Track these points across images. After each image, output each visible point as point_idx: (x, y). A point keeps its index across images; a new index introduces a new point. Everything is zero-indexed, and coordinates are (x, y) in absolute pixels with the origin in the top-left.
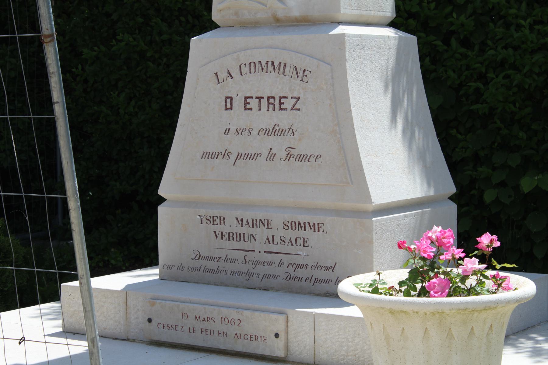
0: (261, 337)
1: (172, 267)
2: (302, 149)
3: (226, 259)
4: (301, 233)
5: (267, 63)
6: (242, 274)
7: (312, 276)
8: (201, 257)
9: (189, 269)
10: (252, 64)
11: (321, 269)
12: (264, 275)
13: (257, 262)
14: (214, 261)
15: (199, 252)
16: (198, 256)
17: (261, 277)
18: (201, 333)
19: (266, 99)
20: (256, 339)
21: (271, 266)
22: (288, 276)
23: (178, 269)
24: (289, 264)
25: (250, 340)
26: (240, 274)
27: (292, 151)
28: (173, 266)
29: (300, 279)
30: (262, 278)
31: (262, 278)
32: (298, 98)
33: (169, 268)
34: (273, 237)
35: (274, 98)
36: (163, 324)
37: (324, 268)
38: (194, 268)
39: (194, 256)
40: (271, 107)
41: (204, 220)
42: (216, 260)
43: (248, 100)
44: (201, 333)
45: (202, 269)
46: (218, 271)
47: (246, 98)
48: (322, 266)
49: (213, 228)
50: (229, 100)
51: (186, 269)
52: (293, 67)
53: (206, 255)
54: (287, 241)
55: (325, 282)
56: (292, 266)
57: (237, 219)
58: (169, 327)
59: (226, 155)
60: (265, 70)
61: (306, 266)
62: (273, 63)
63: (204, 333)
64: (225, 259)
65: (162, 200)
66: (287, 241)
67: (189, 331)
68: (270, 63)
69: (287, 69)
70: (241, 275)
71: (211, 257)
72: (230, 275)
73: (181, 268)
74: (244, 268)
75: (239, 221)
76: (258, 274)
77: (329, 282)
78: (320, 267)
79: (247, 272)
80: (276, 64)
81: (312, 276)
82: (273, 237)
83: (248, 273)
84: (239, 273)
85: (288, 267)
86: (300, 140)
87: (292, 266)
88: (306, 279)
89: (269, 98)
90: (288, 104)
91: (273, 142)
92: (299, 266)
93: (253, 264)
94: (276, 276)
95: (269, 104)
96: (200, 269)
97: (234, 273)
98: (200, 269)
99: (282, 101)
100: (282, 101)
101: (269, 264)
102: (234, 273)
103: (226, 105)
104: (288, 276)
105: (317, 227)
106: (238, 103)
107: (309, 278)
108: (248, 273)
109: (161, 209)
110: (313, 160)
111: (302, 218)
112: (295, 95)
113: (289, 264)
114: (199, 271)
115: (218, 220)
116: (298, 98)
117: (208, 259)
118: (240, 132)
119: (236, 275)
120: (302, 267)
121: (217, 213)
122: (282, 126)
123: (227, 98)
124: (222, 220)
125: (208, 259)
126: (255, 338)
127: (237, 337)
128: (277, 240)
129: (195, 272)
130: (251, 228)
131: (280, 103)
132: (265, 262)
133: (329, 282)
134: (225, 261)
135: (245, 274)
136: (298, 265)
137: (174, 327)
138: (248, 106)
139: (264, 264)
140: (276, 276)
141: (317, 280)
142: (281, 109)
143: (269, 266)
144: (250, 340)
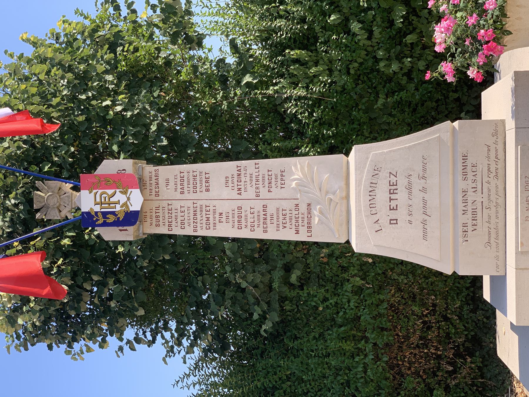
2: (419, 168)
4: (469, 168)
5: (370, 195)
10: (371, 206)
17: (498, 197)
19: (391, 195)
26: (497, 212)
27: (421, 175)
29: (497, 169)
32: (390, 173)
34: (472, 188)
35: (390, 190)
39: (489, 247)
40: (395, 191)
41: (466, 239)
42: (490, 230)
43: (392, 208)
45: (496, 241)
46: (496, 229)
47: (390, 210)
49: (470, 233)
50: (392, 222)
52: (373, 178)
53: (487, 238)
54: (474, 178)
57: (463, 214)
59: (424, 222)
60: (374, 197)
62: (370, 192)
65: (454, 272)
66: (474, 178)
68: (371, 194)
69: (374, 182)
74: (493, 209)
75: (465, 212)
80: (371, 189)
82: (472, 188)
86: (414, 171)
89: (390, 194)
90: (393, 179)
91: (415, 190)
92: (489, 170)
95: (393, 193)
99: (392, 184)
100: (392, 184)
103: (395, 224)
105: (465, 158)
106: (393, 215)
109: (461, 273)
110: (425, 162)
111: (460, 168)
112: (388, 175)
115: (465, 228)
116: (390, 173)
118: (411, 213)
121: (460, 229)
122: (406, 183)
123: (390, 223)
124: (465, 225)
128: (474, 185)
130: (468, 204)
131: (393, 185)
138: (395, 208)
142: (396, 185)
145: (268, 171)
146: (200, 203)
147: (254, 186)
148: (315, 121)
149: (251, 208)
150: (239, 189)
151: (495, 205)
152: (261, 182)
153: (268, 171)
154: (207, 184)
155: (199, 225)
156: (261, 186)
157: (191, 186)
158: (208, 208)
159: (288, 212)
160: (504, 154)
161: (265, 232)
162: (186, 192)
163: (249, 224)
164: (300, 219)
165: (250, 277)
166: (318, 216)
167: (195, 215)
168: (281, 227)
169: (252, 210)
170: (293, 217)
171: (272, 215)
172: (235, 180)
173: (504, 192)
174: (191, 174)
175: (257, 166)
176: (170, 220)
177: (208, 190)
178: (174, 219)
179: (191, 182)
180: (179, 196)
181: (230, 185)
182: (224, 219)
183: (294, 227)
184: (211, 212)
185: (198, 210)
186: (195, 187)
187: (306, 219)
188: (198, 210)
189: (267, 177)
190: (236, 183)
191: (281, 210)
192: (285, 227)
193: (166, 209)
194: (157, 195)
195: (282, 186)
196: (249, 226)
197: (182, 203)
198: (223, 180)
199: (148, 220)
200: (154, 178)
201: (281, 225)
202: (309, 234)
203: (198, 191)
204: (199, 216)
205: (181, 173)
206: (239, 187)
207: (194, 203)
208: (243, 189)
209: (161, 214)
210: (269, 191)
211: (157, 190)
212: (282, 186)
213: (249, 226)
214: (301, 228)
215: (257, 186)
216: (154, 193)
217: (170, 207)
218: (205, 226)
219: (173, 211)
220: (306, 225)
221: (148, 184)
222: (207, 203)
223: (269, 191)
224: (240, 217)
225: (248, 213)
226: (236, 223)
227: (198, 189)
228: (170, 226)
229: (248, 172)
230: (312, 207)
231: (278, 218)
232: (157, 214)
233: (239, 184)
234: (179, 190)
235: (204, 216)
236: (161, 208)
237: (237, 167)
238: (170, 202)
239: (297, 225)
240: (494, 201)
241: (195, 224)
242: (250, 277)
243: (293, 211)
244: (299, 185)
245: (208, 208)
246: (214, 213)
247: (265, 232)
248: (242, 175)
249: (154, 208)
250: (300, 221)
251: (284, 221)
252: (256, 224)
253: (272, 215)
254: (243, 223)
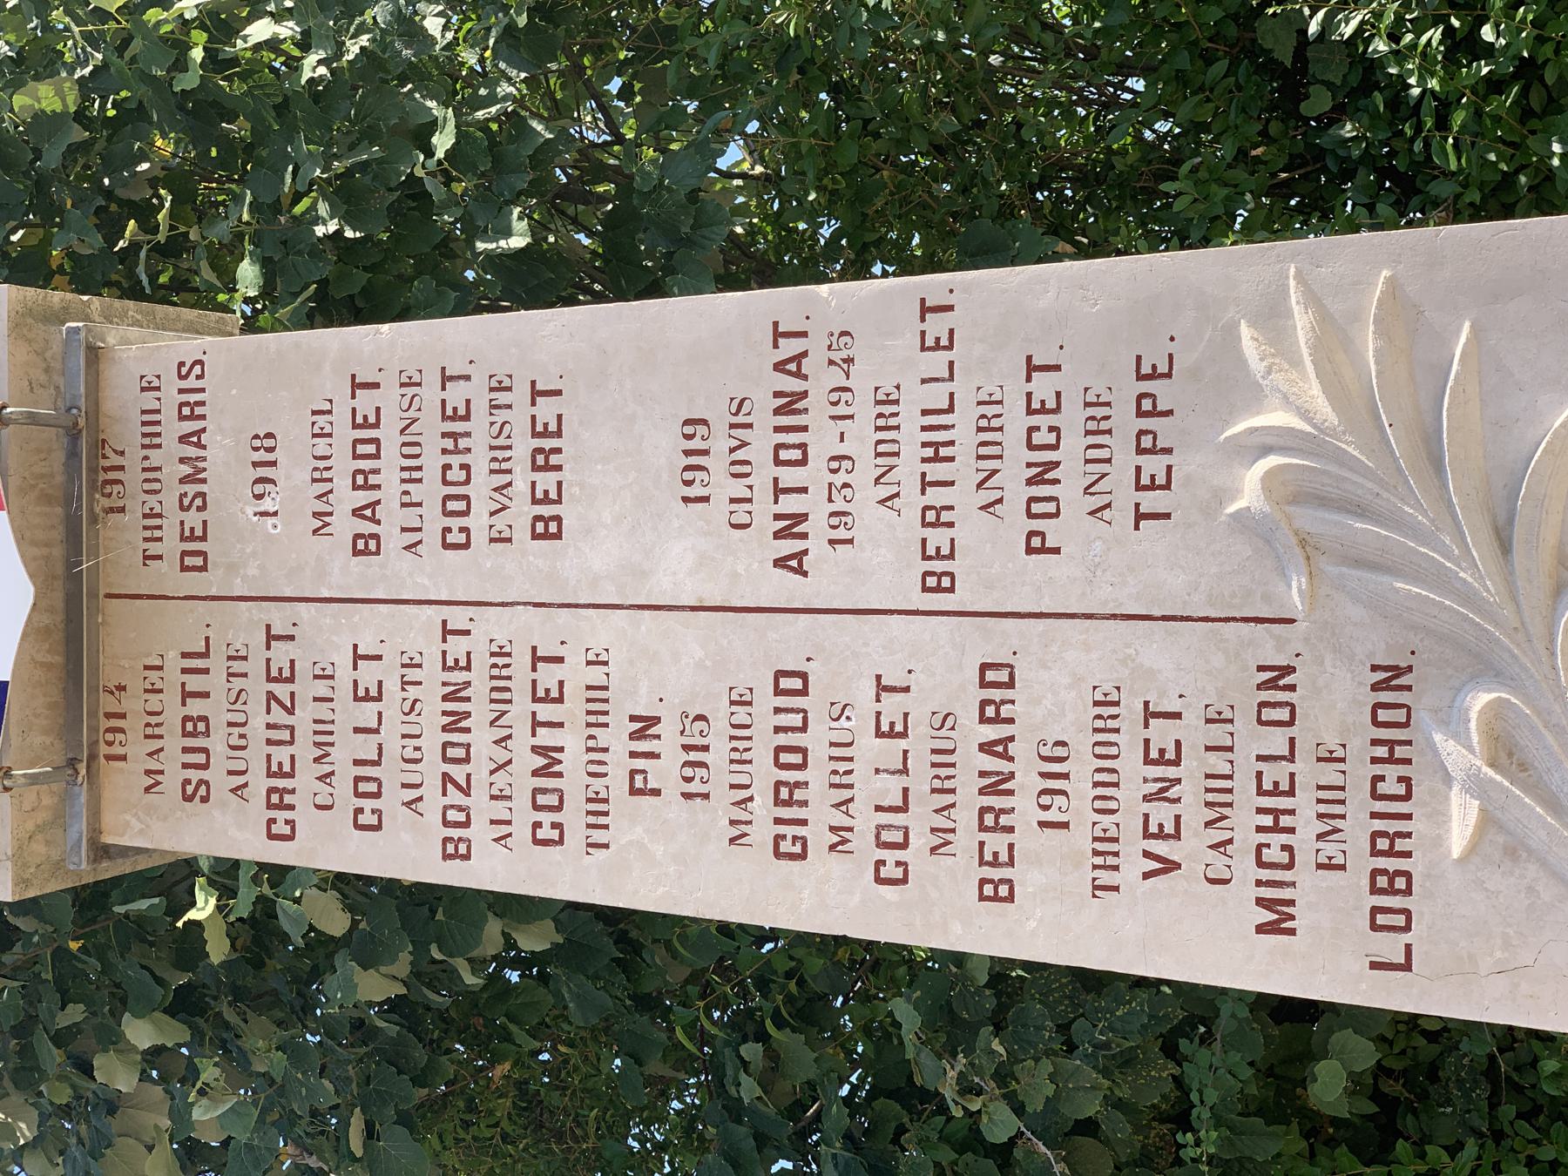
145: (1031, 368)
146: (490, 627)
147: (912, 500)
148: (1495, 85)
149: (882, 688)
150: (791, 525)
152: (964, 469)
153: (1031, 368)
154: (547, 481)
155: (479, 802)
156: (964, 498)
157: (430, 491)
158: (548, 677)
159: (1193, 731)
161: (998, 893)
162: (393, 540)
163: (864, 821)
164: (1305, 804)
165: (1037, 1085)
166: (1476, 787)
167: (455, 723)
168: (1133, 865)
169: (892, 706)
170: (1244, 786)
171: (1055, 757)
172: (761, 444)
174: (430, 394)
175: (937, 326)
176: (281, 755)
177: (548, 530)
178: (304, 750)
179: (432, 461)
180: (347, 574)
181: (723, 486)
182: (666, 771)
183: (1245, 869)
184: (574, 708)
185: (480, 685)
186: (456, 504)
187: (1358, 803)
188: (480, 685)
189: (1015, 422)
190: (764, 473)
191: (1131, 709)
192: (1170, 866)
193: (255, 667)
194: (195, 561)
195: (1150, 502)
196: (863, 840)
197: (368, 628)
198: (666, 447)
199: (137, 748)
200: (172, 428)
201: (1132, 848)
202: (1390, 947)
203: (479, 538)
204: (481, 738)
205: (356, 386)
206: (790, 504)
207: (446, 632)
208: (818, 526)
209: (216, 710)
210: (1037, 546)
211: (193, 519)
212: (1150, 502)
213: (863, 840)
214: (1307, 886)
215: (936, 496)
216: (171, 545)
217: (281, 654)
218: (523, 816)
219: (306, 688)
220: (1362, 864)
221: (133, 477)
222: (543, 631)
223: (1037, 546)
224: (791, 757)
225: (860, 724)
226: (762, 807)
227: (478, 521)
228: (278, 800)
229: (862, 381)
230: (1423, 702)
231: (1106, 781)
232: (195, 707)
233: (789, 477)
234: (345, 526)
235: (522, 740)
236: (217, 663)
237: (778, 335)
238: (279, 618)
239: (1273, 854)
241: (455, 797)
242: (1037, 1085)
243: (1244, 724)
244: (1298, 498)
245: (548, 677)
246: (597, 718)
247: (998, 893)
248: (817, 402)
249: (174, 663)
250: (1307, 826)
251: (1162, 814)
252: (919, 821)
253: (1055, 757)
254: (820, 814)
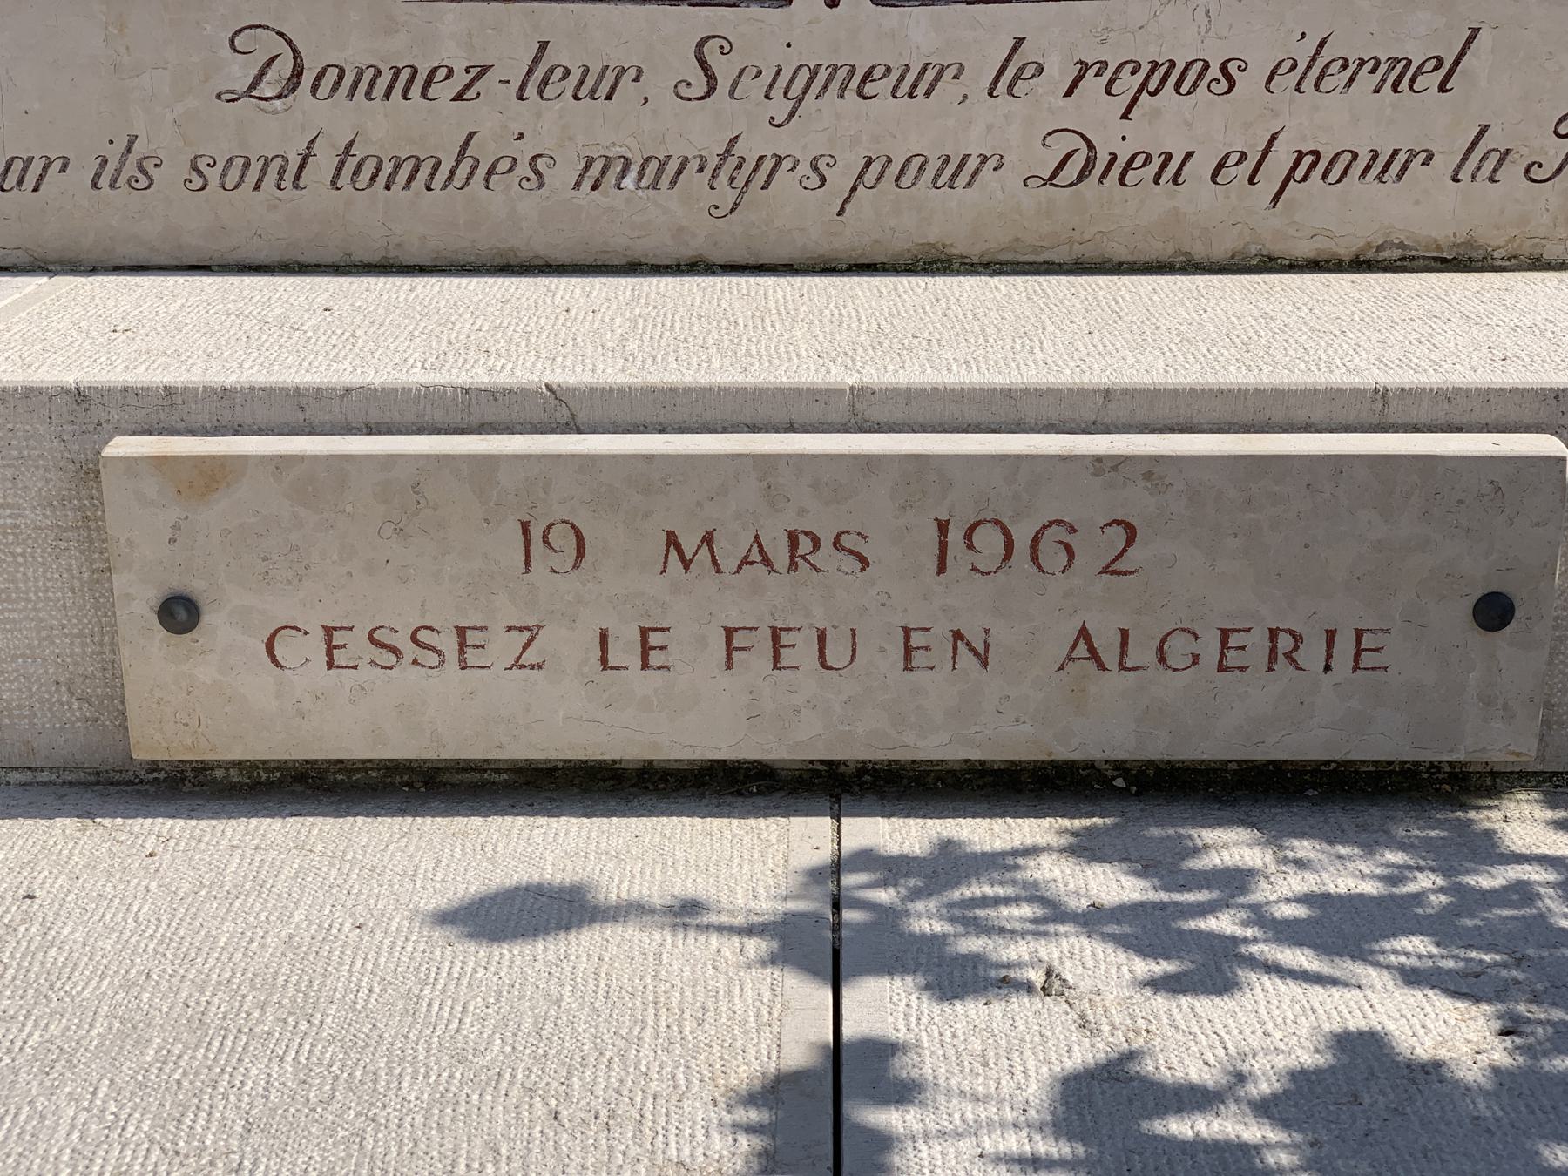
0: (1331, 635)
1: (46, 168)
3: (539, 73)
6: (679, 172)
7: (1274, 138)
8: (308, 79)
9: (200, 173)
11: (1352, 80)
12: (868, 165)
13: (804, 74)
14: (424, 95)
15: (290, 42)
16: (284, 67)
17: (840, 180)
18: (729, 666)
20: (1281, 657)
21: (927, 94)
22: (1069, 156)
23: (104, 182)
24: (1084, 67)
25: (1222, 668)
28: (58, 165)
30: (854, 189)
31: (854, 189)
33: (20, 182)
36: (329, 631)
37: (1373, 71)
38: (247, 165)
39: (239, 74)
42: (443, 91)
44: (729, 666)
45: (324, 162)
48: (1362, 63)
51: (170, 175)
53: (354, 55)
55: (1375, 171)
56: (1111, 82)
58: (394, 650)
61: (1224, 68)
63: (756, 661)
64: (530, 72)
67: (604, 660)
70: (673, 183)
71: (397, 72)
72: (577, 185)
73: (130, 169)
76: (814, 166)
77: (1405, 167)
78: (1345, 66)
79: (723, 158)
81: (1274, 138)
83: (732, 162)
84: (653, 166)
85: (1069, 93)
87: (1111, 82)
88: (1221, 166)
93: (777, 92)
94: (972, 164)
96: (301, 167)
97: (604, 172)
98: (301, 167)
101: (914, 86)
102: (604, 172)
104: (1069, 156)
107: (1243, 156)
108: (732, 162)
113: (1084, 67)
114: (297, 177)
117: (372, 85)
119: (629, 182)
120: (1195, 85)
125: (372, 85)
126: (1273, 650)
127: (1094, 655)
129: (257, 187)
132: (877, 74)
133: (1405, 167)
134: (531, 91)
135: (708, 171)
136: (1155, 66)
137: (449, 644)
139: (869, 89)
140: (972, 164)
141: (1308, 160)
143: (911, 96)
144: (1222, 668)
151: (749, 149)
160: (1345, 251)
173: (897, 246)
240: (798, 142)
